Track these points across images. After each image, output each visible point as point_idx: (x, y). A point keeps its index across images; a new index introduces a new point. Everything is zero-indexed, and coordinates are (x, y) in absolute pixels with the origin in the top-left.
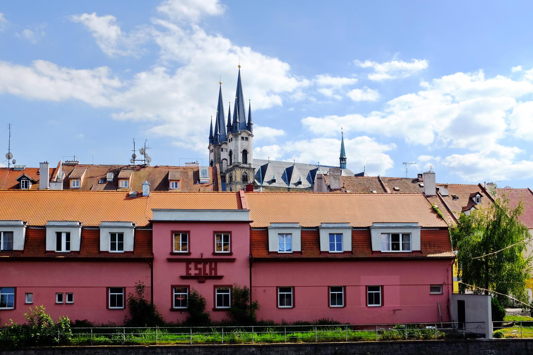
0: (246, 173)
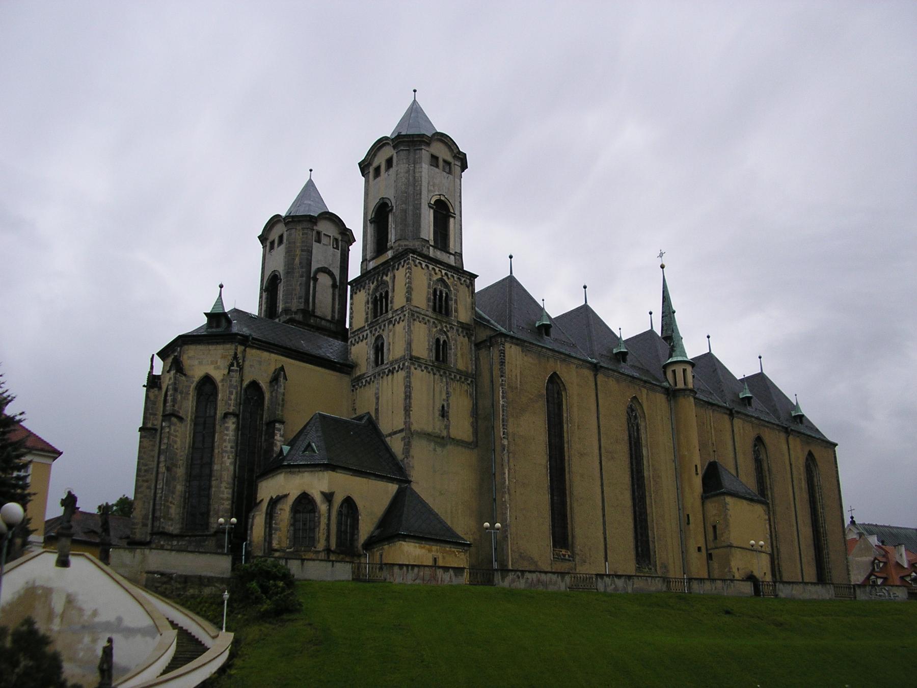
0: (446, 286)
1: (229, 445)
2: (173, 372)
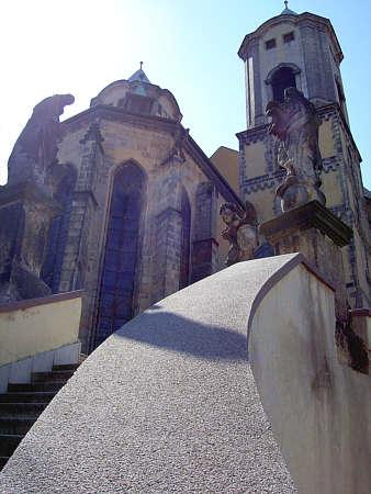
1: (174, 251)
2: (90, 143)
